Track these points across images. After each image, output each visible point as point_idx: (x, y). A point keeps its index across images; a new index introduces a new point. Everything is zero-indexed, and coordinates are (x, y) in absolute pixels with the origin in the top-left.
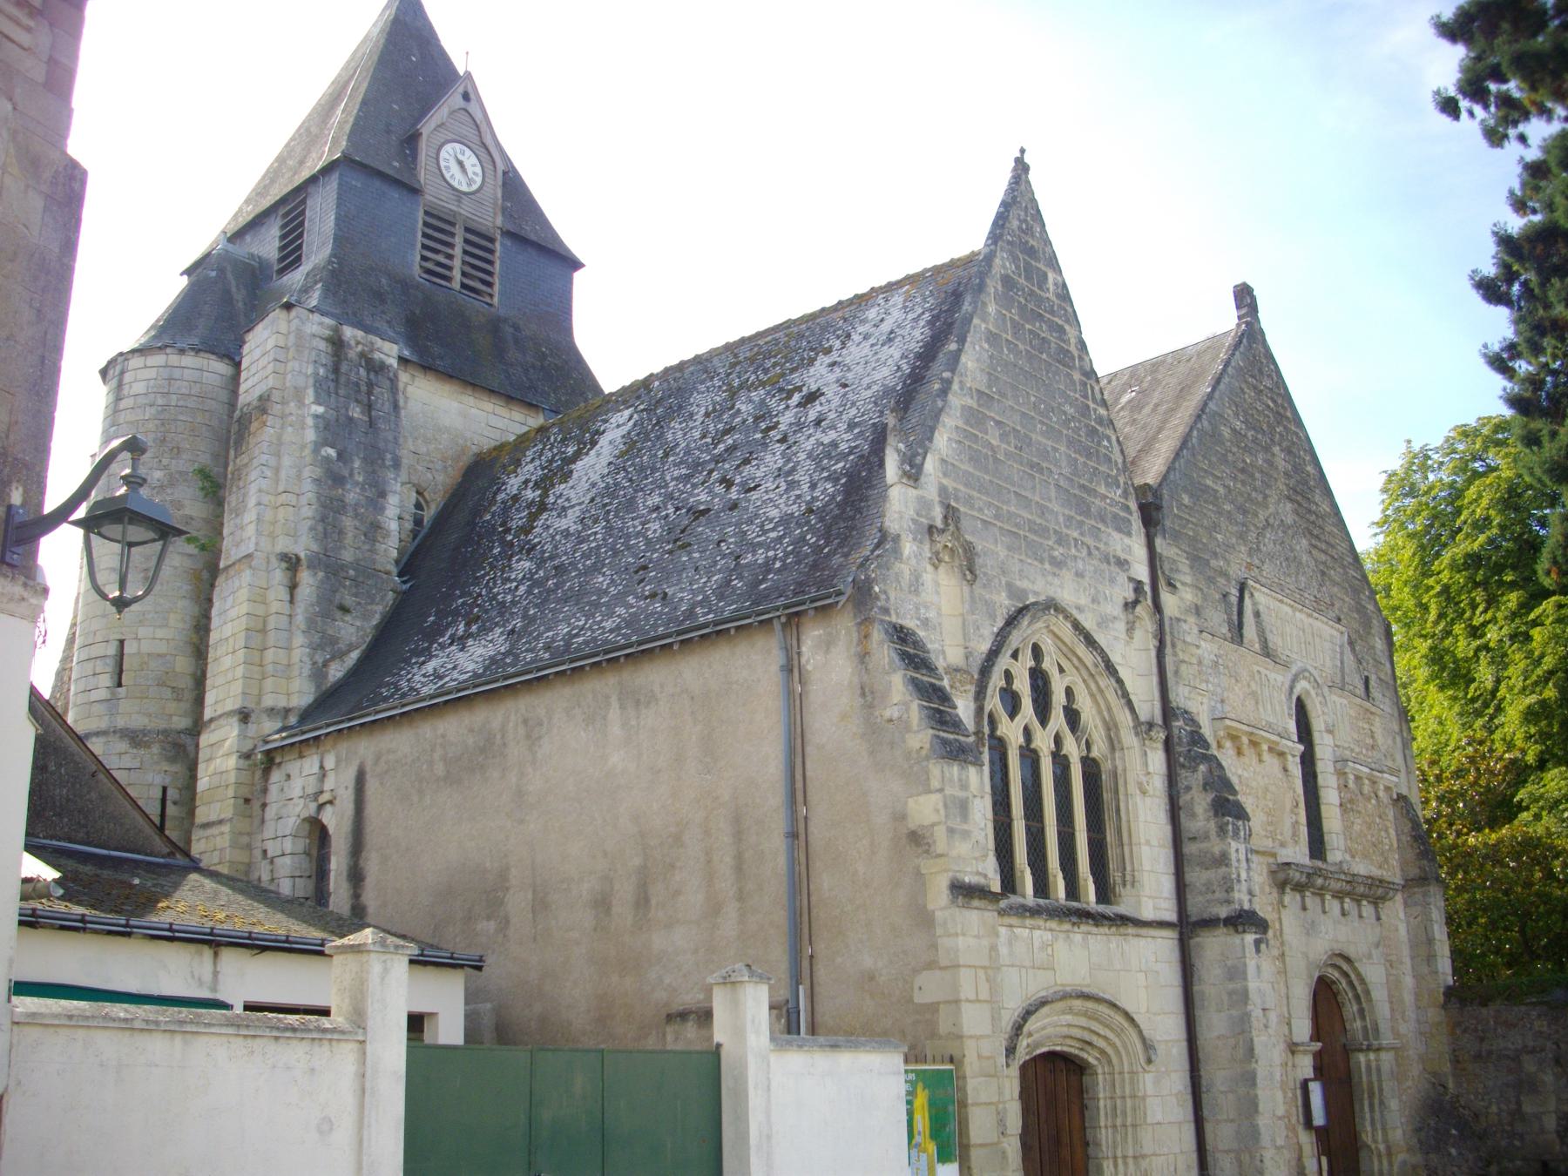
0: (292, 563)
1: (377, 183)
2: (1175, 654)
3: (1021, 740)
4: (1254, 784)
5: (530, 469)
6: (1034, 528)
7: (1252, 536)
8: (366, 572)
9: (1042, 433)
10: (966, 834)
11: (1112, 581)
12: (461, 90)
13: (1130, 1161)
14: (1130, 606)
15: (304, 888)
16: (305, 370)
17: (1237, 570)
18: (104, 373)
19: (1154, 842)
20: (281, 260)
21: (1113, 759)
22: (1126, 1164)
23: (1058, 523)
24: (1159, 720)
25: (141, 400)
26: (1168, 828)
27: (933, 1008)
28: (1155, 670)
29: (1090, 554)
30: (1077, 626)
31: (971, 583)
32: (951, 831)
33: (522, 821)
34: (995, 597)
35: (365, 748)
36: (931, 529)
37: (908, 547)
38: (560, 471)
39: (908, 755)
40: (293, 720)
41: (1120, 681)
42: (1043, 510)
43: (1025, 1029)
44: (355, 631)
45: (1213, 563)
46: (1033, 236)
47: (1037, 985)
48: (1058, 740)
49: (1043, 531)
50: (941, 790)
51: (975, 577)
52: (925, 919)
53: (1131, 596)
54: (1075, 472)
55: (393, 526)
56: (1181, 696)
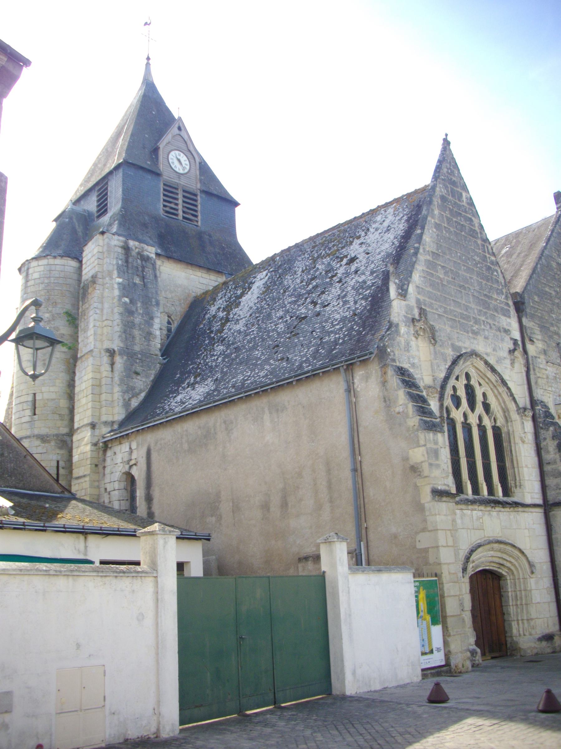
0: (111, 353)
1: (141, 172)
2: (535, 374)
3: (462, 419)
5: (220, 302)
6: (463, 317)
8: (146, 355)
9: (465, 271)
10: (438, 466)
11: (502, 340)
12: (177, 126)
13: (525, 622)
14: (512, 352)
15: (125, 505)
16: (112, 262)
18: (20, 270)
19: (530, 466)
20: (98, 211)
21: (508, 427)
22: (523, 623)
23: (474, 313)
24: (529, 406)
25: (38, 281)
26: (536, 459)
27: (426, 550)
28: (525, 382)
29: (491, 328)
30: (486, 363)
31: (434, 345)
32: (431, 465)
33: (225, 469)
34: (446, 351)
35: (150, 438)
36: (413, 320)
37: (403, 329)
38: (235, 302)
39: (408, 430)
40: (116, 426)
41: (509, 389)
42: (467, 308)
43: (471, 559)
44: (142, 384)
45: (552, 329)
46: (454, 176)
47: (475, 538)
48: (480, 418)
49: (467, 318)
50: (425, 445)
51: (436, 342)
52: (420, 508)
53: (512, 347)
54: (481, 288)
55: (158, 333)
56: (539, 394)
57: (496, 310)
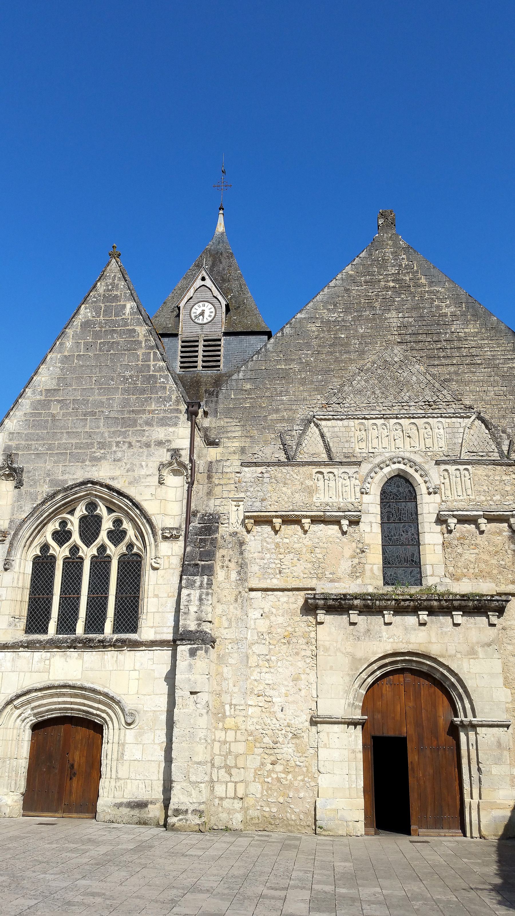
4: (296, 546)
6: (78, 446)
7: (336, 383)
9: (99, 394)
17: (302, 412)
29: (130, 445)
34: (39, 489)
45: (275, 416)
57: (148, 423)
